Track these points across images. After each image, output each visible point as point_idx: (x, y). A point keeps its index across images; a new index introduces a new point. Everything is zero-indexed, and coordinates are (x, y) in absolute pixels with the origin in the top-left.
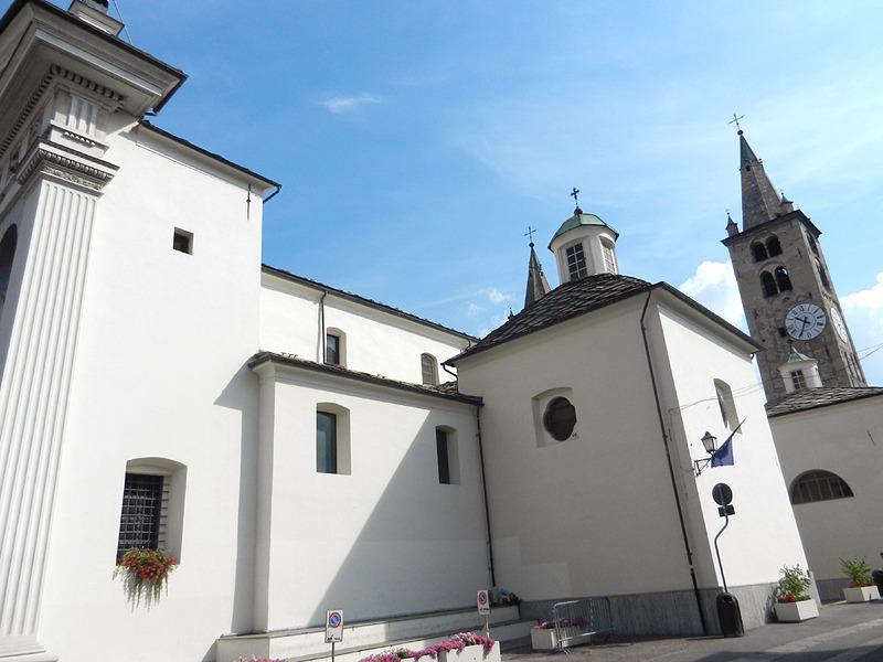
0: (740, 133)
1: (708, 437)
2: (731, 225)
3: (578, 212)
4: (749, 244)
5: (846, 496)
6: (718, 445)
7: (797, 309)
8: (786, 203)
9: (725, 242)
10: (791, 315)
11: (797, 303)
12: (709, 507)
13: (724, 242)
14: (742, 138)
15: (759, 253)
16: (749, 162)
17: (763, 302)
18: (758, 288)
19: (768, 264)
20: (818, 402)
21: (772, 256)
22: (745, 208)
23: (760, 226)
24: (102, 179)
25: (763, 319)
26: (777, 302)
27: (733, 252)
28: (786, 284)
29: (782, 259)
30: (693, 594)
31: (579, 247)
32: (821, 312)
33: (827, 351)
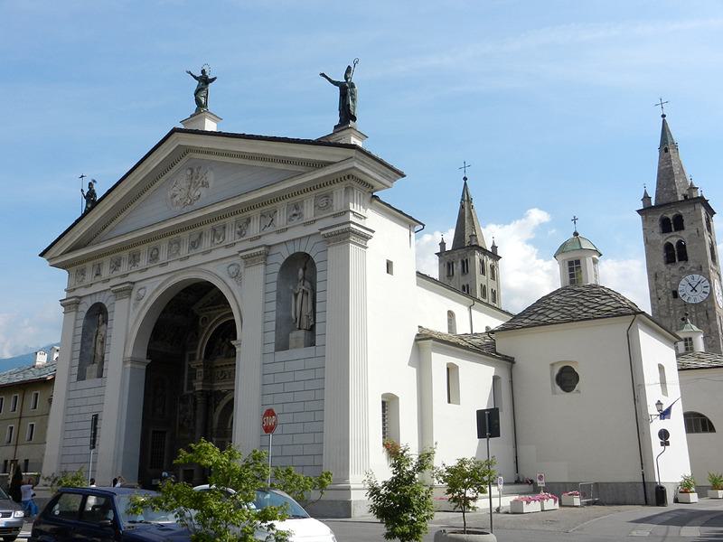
0: (664, 116)
1: (659, 403)
2: (646, 198)
3: (576, 234)
4: (659, 217)
5: (705, 430)
6: (664, 409)
7: (689, 277)
8: (692, 188)
9: (639, 212)
10: (683, 282)
11: (690, 272)
12: (656, 440)
13: (639, 211)
14: (664, 121)
15: (666, 226)
16: (666, 144)
17: (663, 267)
18: (661, 255)
19: (671, 237)
20: (701, 364)
21: (676, 230)
22: (659, 183)
23: (669, 204)
24: (367, 238)
25: (661, 281)
26: (674, 269)
27: (644, 221)
28: (683, 256)
29: (684, 235)
30: (642, 487)
31: (578, 262)
32: (707, 283)
33: (707, 314)
